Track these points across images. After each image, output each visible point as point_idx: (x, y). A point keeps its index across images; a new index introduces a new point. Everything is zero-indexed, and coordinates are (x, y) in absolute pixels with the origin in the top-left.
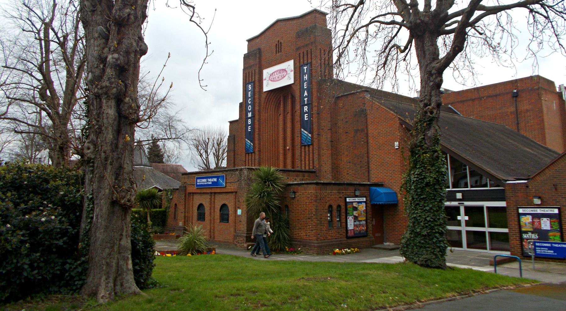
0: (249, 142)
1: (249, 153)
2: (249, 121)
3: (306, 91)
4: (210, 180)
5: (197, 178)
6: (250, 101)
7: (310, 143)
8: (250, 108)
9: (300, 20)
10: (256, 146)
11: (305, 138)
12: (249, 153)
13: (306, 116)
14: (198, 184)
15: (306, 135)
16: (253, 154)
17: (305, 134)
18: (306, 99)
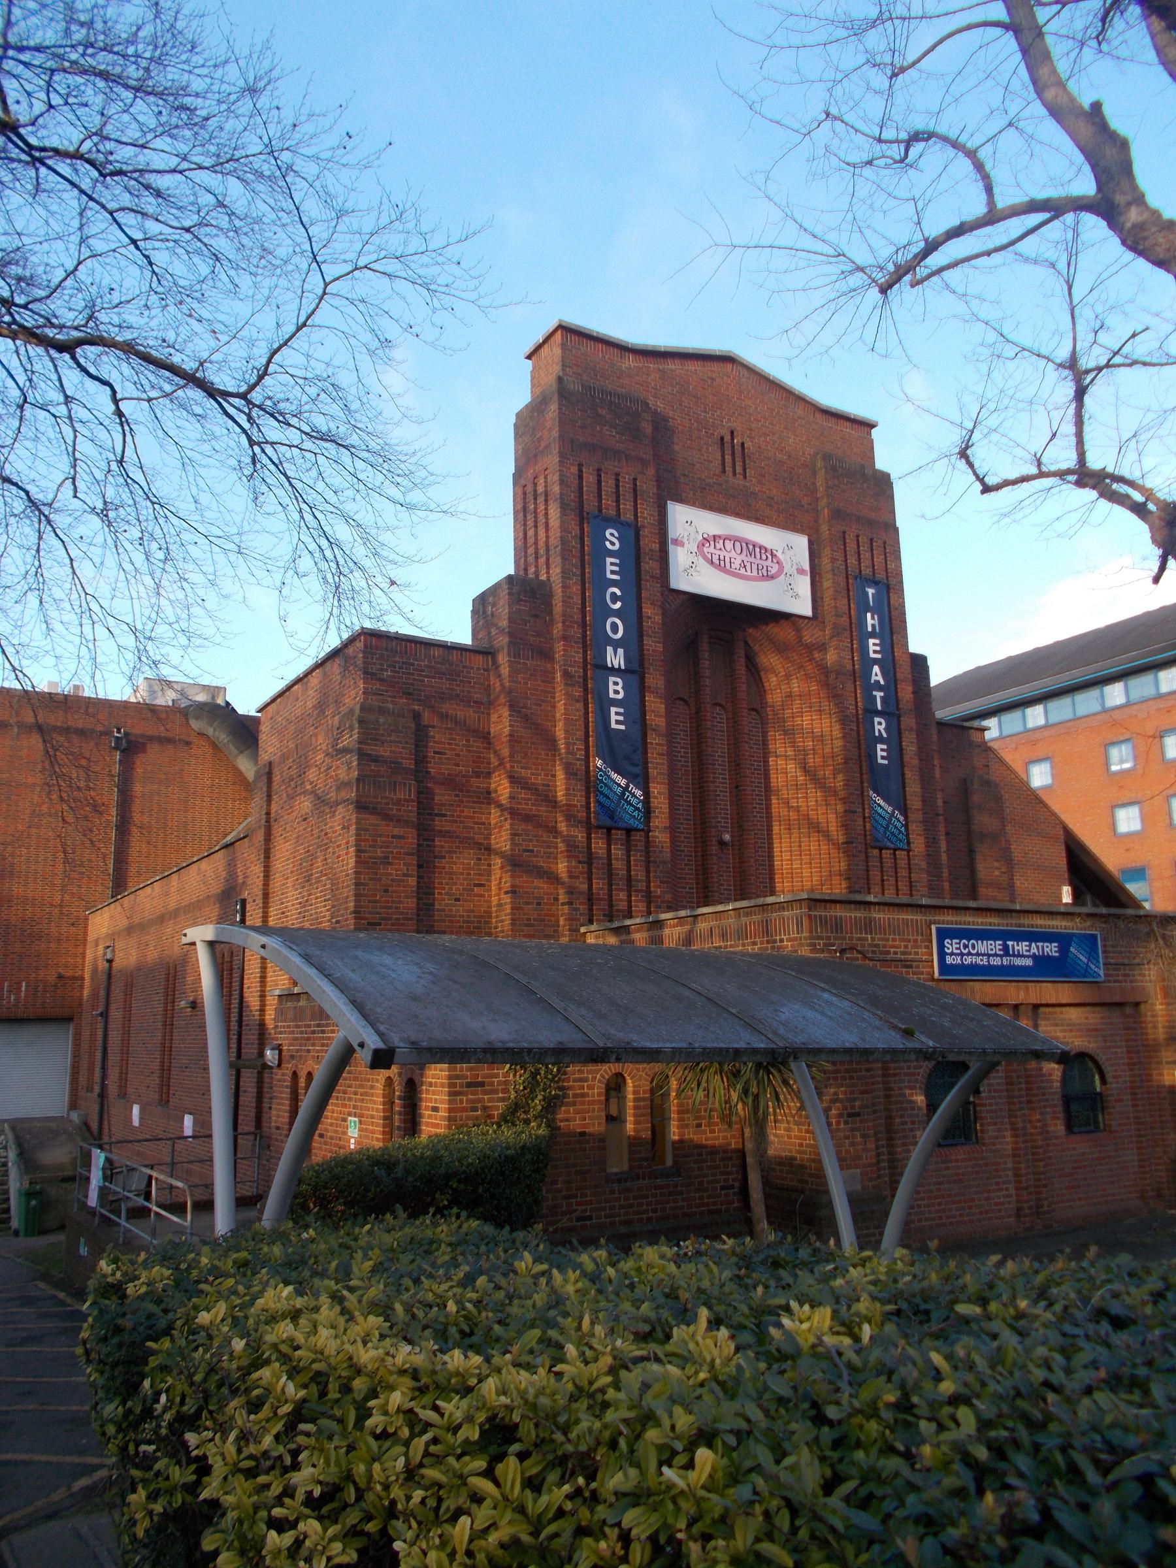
0: (614, 776)
1: (609, 830)
2: (616, 688)
3: (876, 669)
4: (1022, 947)
5: (943, 935)
6: (615, 599)
7: (901, 845)
8: (616, 628)
9: (821, 420)
10: (654, 802)
11: (884, 823)
12: (609, 830)
13: (881, 750)
14: (949, 960)
15: (883, 814)
16: (638, 837)
17: (879, 810)
18: (879, 695)
